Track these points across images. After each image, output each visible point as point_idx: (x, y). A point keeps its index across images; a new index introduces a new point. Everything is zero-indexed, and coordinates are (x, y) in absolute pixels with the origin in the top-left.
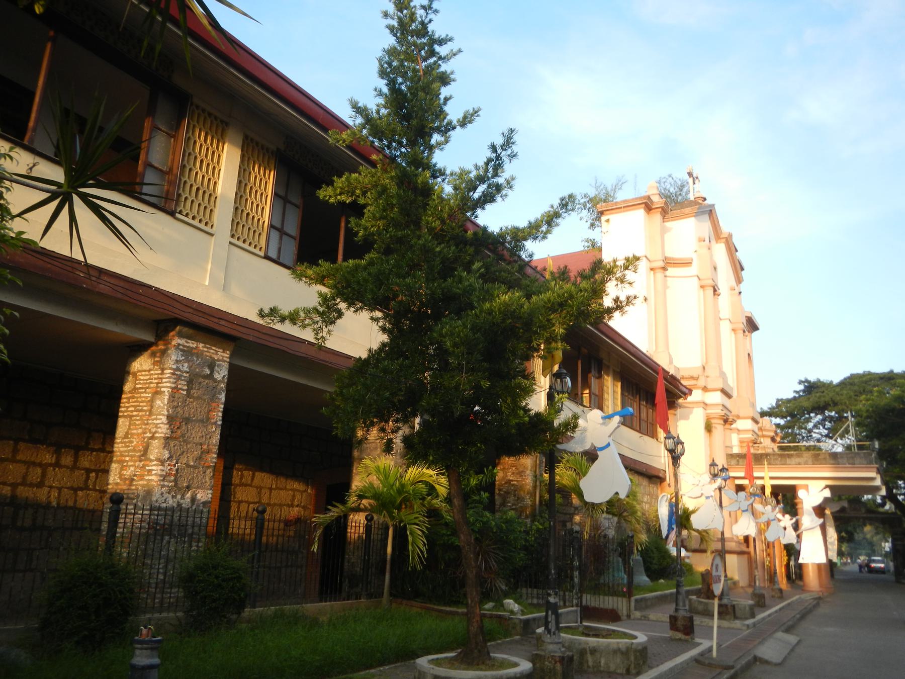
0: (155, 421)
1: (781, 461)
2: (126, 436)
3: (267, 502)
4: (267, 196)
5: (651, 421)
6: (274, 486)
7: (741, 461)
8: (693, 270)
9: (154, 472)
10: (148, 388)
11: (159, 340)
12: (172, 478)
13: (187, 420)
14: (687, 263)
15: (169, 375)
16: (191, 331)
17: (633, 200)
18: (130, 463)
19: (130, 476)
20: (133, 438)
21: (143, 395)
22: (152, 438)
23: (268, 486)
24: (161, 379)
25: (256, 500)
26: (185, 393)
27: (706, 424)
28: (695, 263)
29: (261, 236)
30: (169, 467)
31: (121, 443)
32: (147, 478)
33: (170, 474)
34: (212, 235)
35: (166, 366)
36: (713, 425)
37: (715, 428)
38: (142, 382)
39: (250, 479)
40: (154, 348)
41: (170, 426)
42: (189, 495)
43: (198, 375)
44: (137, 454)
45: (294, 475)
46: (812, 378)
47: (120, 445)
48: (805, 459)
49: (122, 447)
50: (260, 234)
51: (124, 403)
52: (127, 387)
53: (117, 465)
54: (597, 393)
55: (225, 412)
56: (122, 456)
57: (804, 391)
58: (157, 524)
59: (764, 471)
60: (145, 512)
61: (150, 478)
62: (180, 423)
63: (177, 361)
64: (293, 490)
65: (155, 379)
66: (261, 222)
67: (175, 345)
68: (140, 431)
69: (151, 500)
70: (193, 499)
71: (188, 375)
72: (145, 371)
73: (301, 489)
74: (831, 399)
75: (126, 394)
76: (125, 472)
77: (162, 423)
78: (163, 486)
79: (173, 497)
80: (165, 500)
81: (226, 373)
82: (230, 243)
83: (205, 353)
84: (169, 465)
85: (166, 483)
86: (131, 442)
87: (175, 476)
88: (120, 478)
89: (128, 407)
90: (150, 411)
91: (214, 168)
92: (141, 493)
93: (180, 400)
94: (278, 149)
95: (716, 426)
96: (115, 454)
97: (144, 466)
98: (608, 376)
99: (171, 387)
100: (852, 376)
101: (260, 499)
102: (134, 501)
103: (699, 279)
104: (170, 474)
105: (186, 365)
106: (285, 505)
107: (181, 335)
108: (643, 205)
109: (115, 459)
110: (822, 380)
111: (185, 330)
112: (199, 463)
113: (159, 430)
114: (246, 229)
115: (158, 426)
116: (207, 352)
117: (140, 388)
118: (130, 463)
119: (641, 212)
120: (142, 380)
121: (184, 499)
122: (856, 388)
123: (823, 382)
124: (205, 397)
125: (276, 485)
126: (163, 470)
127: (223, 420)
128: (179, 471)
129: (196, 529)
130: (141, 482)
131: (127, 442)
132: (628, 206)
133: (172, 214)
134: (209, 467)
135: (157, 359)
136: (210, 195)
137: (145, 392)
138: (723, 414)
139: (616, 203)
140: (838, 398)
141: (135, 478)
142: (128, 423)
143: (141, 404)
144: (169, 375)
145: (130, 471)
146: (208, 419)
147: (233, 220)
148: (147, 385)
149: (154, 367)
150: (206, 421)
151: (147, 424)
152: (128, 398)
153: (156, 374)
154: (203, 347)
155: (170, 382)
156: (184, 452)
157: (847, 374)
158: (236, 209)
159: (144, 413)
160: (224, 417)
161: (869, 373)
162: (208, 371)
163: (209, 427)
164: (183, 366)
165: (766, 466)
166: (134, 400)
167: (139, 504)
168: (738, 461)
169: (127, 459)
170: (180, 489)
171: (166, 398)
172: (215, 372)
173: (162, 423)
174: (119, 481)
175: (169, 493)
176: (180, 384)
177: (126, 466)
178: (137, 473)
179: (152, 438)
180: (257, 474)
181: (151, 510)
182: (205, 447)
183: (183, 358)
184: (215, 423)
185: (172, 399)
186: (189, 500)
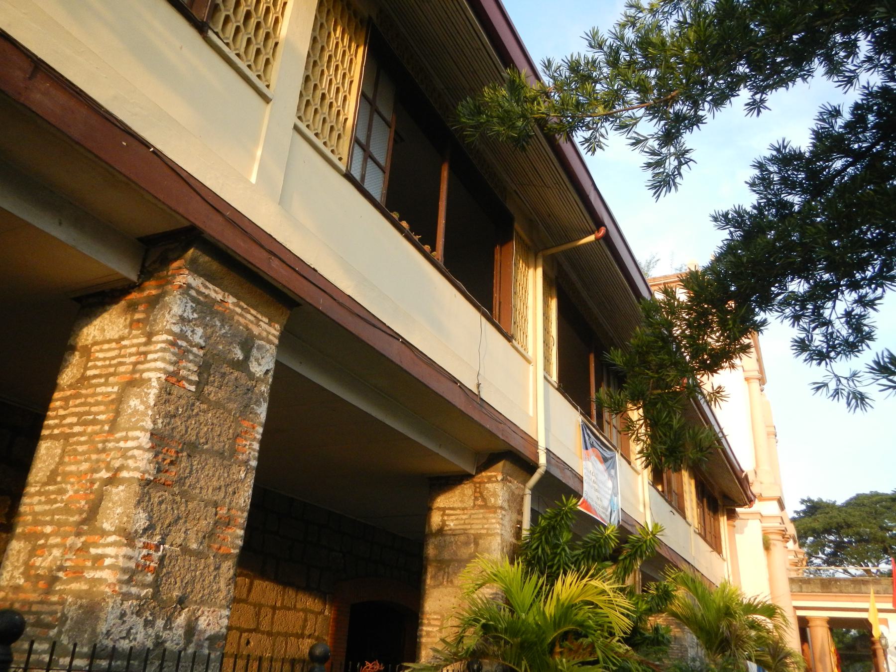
0: (122, 444)
1: (854, 588)
2: (52, 479)
3: (267, 629)
4: (351, 82)
6: (279, 604)
7: (804, 586)
9: (108, 562)
10: (112, 374)
11: (148, 279)
12: (150, 578)
13: (192, 448)
15: (163, 345)
16: (215, 266)
18: (53, 541)
19: (50, 570)
20: (66, 483)
21: (99, 390)
22: (112, 481)
23: (271, 603)
24: (145, 354)
25: (252, 627)
26: (193, 388)
29: (341, 141)
30: (145, 552)
31: (39, 493)
32: (89, 574)
34: (267, 99)
35: (157, 328)
36: (772, 542)
37: (774, 545)
38: (99, 363)
39: (245, 590)
40: (134, 296)
41: (156, 456)
42: (181, 620)
44: (72, 519)
45: (307, 588)
46: (815, 498)
47: (36, 499)
48: (885, 586)
49: (40, 503)
50: (339, 136)
51: (56, 409)
52: (66, 377)
53: (22, 544)
54: (676, 491)
55: (262, 443)
56: (36, 523)
57: (804, 512)
59: (868, 602)
61: (98, 574)
62: (177, 453)
63: (183, 320)
64: (305, 611)
65: (131, 355)
66: (342, 118)
67: (180, 287)
68: (85, 466)
69: (94, 631)
70: (191, 630)
71: (201, 353)
72: (109, 341)
73: (316, 610)
75: (63, 390)
76: (38, 561)
77: (139, 448)
78: (126, 596)
79: (148, 624)
80: (129, 632)
81: (272, 366)
82: (296, 128)
83: (236, 317)
84: (146, 546)
85: (134, 590)
86: (62, 492)
87: (157, 572)
88: (26, 574)
89: (64, 417)
90: (114, 424)
92: (72, 613)
93: (183, 402)
94: (370, 18)
95: (775, 542)
96: (21, 519)
97: (85, 548)
99: (165, 371)
100: (858, 497)
101: (258, 624)
102: (53, 633)
103: (744, 371)
104: (146, 567)
105: (200, 331)
106: (292, 635)
107: (195, 268)
109: (19, 530)
110: (824, 500)
111: (204, 259)
112: (209, 547)
113: (131, 462)
114: (320, 118)
115: (130, 453)
116: (241, 315)
117: (95, 376)
118: (53, 541)
120: (99, 359)
121: (171, 629)
122: (867, 509)
123: (826, 503)
124: (231, 406)
125: (282, 603)
126: (130, 558)
127: (260, 459)
128: (166, 562)
130: (75, 586)
131: (53, 493)
133: (201, 28)
134: (226, 556)
135: (137, 316)
136: (268, 35)
137: (106, 384)
138: (783, 529)
139: (654, 279)
140: (851, 519)
141: (61, 574)
142: (59, 451)
143: (94, 409)
144: (163, 345)
145: (51, 558)
146: (234, 452)
147: (301, 95)
148: (112, 370)
149: (130, 333)
150: (228, 456)
151: (104, 450)
152: (66, 399)
153: (133, 346)
154: (233, 304)
155: (163, 360)
156: (179, 518)
157: (853, 495)
158: (307, 79)
159: (98, 428)
160: (261, 451)
161: (877, 494)
162: (239, 355)
163: (235, 469)
164: (193, 331)
165: (872, 595)
166: (78, 401)
167: (65, 640)
168: (801, 587)
169: (48, 529)
170: (163, 605)
172: (252, 359)
173: (139, 448)
174: (21, 581)
175: (138, 614)
176: (184, 368)
177: (43, 546)
178: (68, 564)
179: (112, 481)
180: (257, 582)
181: (93, 655)
182: (223, 511)
183: (196, 316)
184: (246, 462)
185: (165, 397)
186: (181, 632)
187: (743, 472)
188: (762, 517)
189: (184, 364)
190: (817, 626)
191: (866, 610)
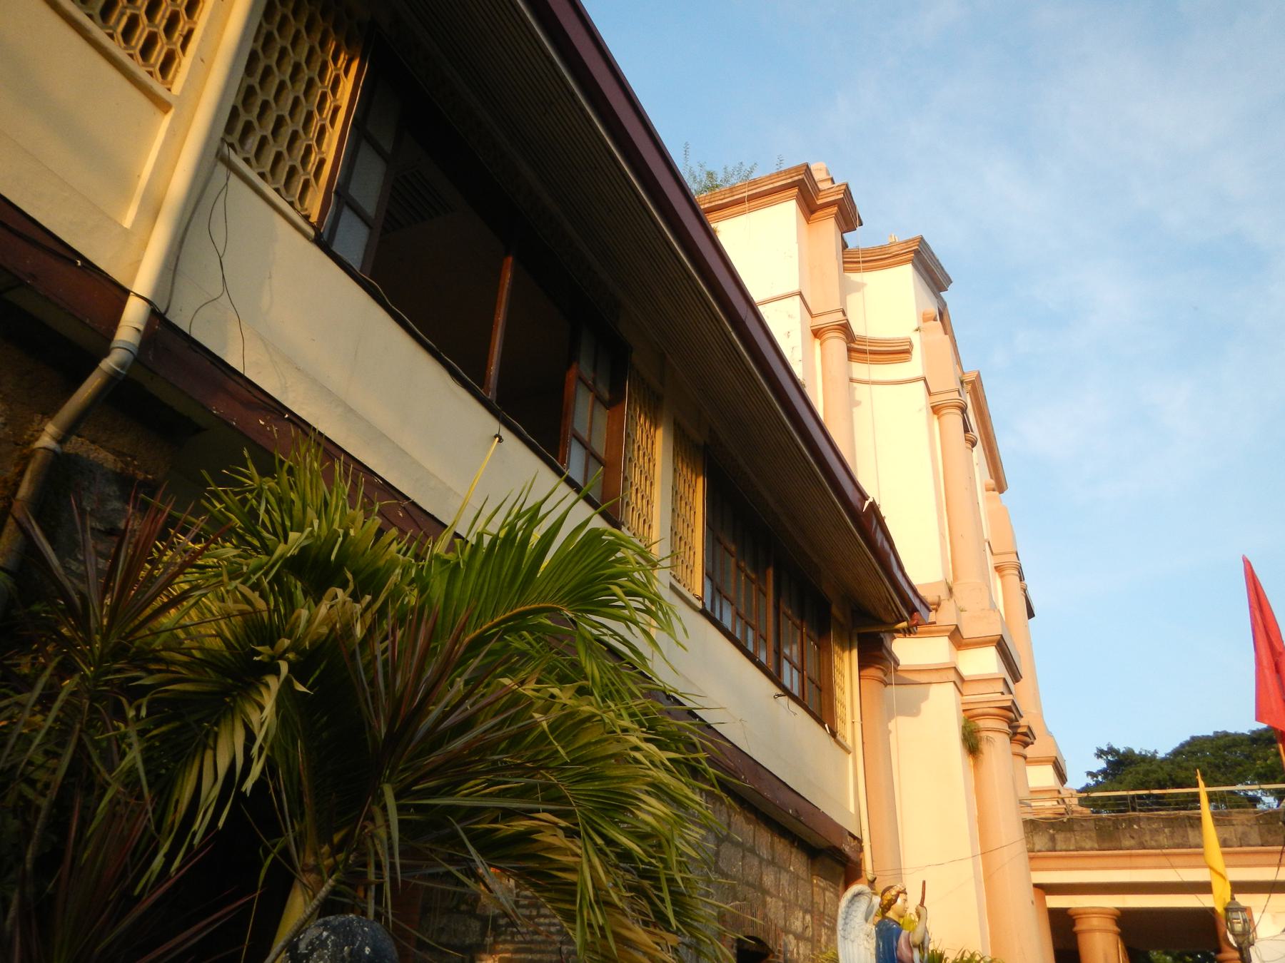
1: (1172, 835)
5: (814, 676)
7: (1059, 837)
8: (913, 367)
14: (900, 352)
17: (770, 177)
27: (964, 728)
28: (917, 352)
36: (984, 734)
46: (1121, 747)
48: (1240, 829)
57: (1103, 772)
74: (1170, 775)
95: (991, 734)
100: (1194, 740)
103: (930, 393)
108: (795, 191)
110: (1137, 752)
119: (788, 210)
132: (760, 196)
138: (1009, 704)
161: (1226, 734)
168: (1053, 839)
187: (864, 497)
188: (961, 681)
190: (1091, 931)
191: (1205, 888)
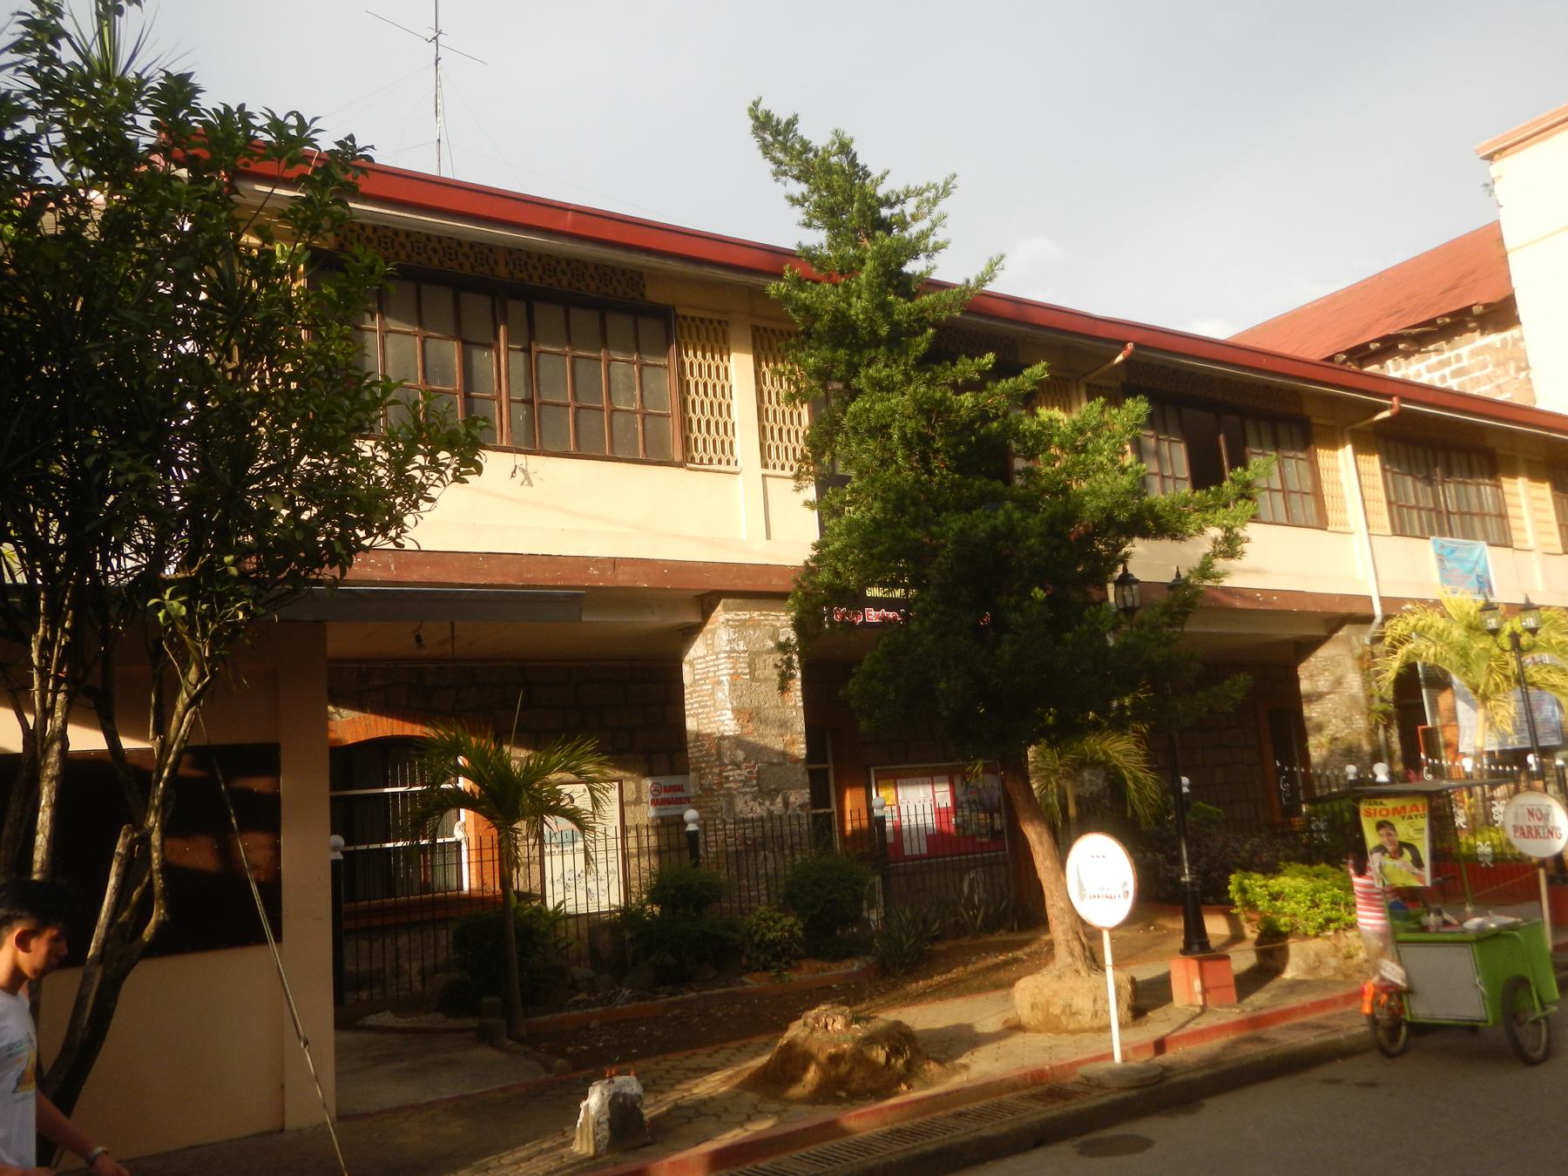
10: (707, 678)
12: (755, 782)
18: (707, 771)
21: (704, 687)
24: (718, 665)
26: (748, 677)
31: (694, 747)
33: (750, 779)
42: (779, 799)
43: (758, 654)
56: (698, 763)
58: (745, 838)
60: (718, 833)
61: (729, 785)
63: (730, 641)
72: (700, 658)
79: (760, 804)
85: (748, 790)
87: (758, 778)
90: (714, 705)
91: (723, 387)
98: (1513, 474)
99: (730, 674)
104: (750, 779)
107: (727, 609)
117: (700, 679)
118: (707, 771)
129: (796, 839)
130: (722, 792)
137: (705, 684)
143: (705, 699)
152: (691, 693)
155: (726, 668)
163: (788, 711)
171: (727, 687)
175: (754, 800)
189: (738, 665)
